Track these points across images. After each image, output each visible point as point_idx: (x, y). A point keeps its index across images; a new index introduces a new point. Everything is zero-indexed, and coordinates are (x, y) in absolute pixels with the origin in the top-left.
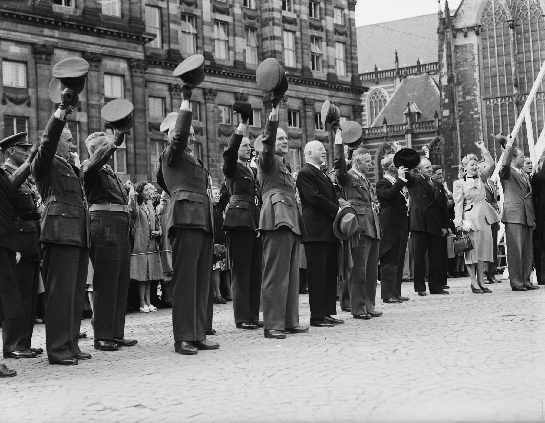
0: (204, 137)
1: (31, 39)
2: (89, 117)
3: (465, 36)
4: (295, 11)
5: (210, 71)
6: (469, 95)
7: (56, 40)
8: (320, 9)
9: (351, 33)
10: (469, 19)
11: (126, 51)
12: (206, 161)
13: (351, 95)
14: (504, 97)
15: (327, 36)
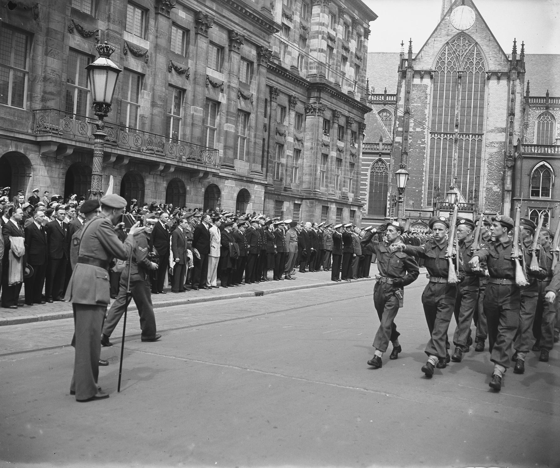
0: (267, 133)
1: (196, 7)
2: (229, 99)
3: (422, 78)
4: (334, 30)
5: (279, 71)
6: (419, 127)
7: (214, 13)
8: (349, 31)
9: (364, 58)
10: (427, 63)
11: (258, 39)
12: (266, 156)
13: (360, 114)
14: (447, 134)
15: (351, 57)
